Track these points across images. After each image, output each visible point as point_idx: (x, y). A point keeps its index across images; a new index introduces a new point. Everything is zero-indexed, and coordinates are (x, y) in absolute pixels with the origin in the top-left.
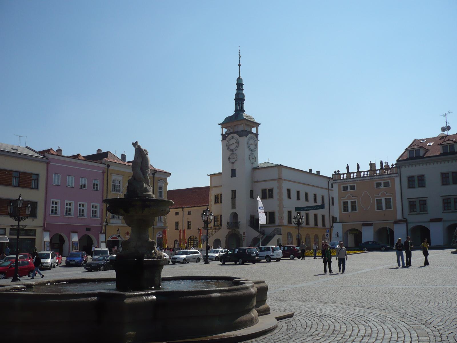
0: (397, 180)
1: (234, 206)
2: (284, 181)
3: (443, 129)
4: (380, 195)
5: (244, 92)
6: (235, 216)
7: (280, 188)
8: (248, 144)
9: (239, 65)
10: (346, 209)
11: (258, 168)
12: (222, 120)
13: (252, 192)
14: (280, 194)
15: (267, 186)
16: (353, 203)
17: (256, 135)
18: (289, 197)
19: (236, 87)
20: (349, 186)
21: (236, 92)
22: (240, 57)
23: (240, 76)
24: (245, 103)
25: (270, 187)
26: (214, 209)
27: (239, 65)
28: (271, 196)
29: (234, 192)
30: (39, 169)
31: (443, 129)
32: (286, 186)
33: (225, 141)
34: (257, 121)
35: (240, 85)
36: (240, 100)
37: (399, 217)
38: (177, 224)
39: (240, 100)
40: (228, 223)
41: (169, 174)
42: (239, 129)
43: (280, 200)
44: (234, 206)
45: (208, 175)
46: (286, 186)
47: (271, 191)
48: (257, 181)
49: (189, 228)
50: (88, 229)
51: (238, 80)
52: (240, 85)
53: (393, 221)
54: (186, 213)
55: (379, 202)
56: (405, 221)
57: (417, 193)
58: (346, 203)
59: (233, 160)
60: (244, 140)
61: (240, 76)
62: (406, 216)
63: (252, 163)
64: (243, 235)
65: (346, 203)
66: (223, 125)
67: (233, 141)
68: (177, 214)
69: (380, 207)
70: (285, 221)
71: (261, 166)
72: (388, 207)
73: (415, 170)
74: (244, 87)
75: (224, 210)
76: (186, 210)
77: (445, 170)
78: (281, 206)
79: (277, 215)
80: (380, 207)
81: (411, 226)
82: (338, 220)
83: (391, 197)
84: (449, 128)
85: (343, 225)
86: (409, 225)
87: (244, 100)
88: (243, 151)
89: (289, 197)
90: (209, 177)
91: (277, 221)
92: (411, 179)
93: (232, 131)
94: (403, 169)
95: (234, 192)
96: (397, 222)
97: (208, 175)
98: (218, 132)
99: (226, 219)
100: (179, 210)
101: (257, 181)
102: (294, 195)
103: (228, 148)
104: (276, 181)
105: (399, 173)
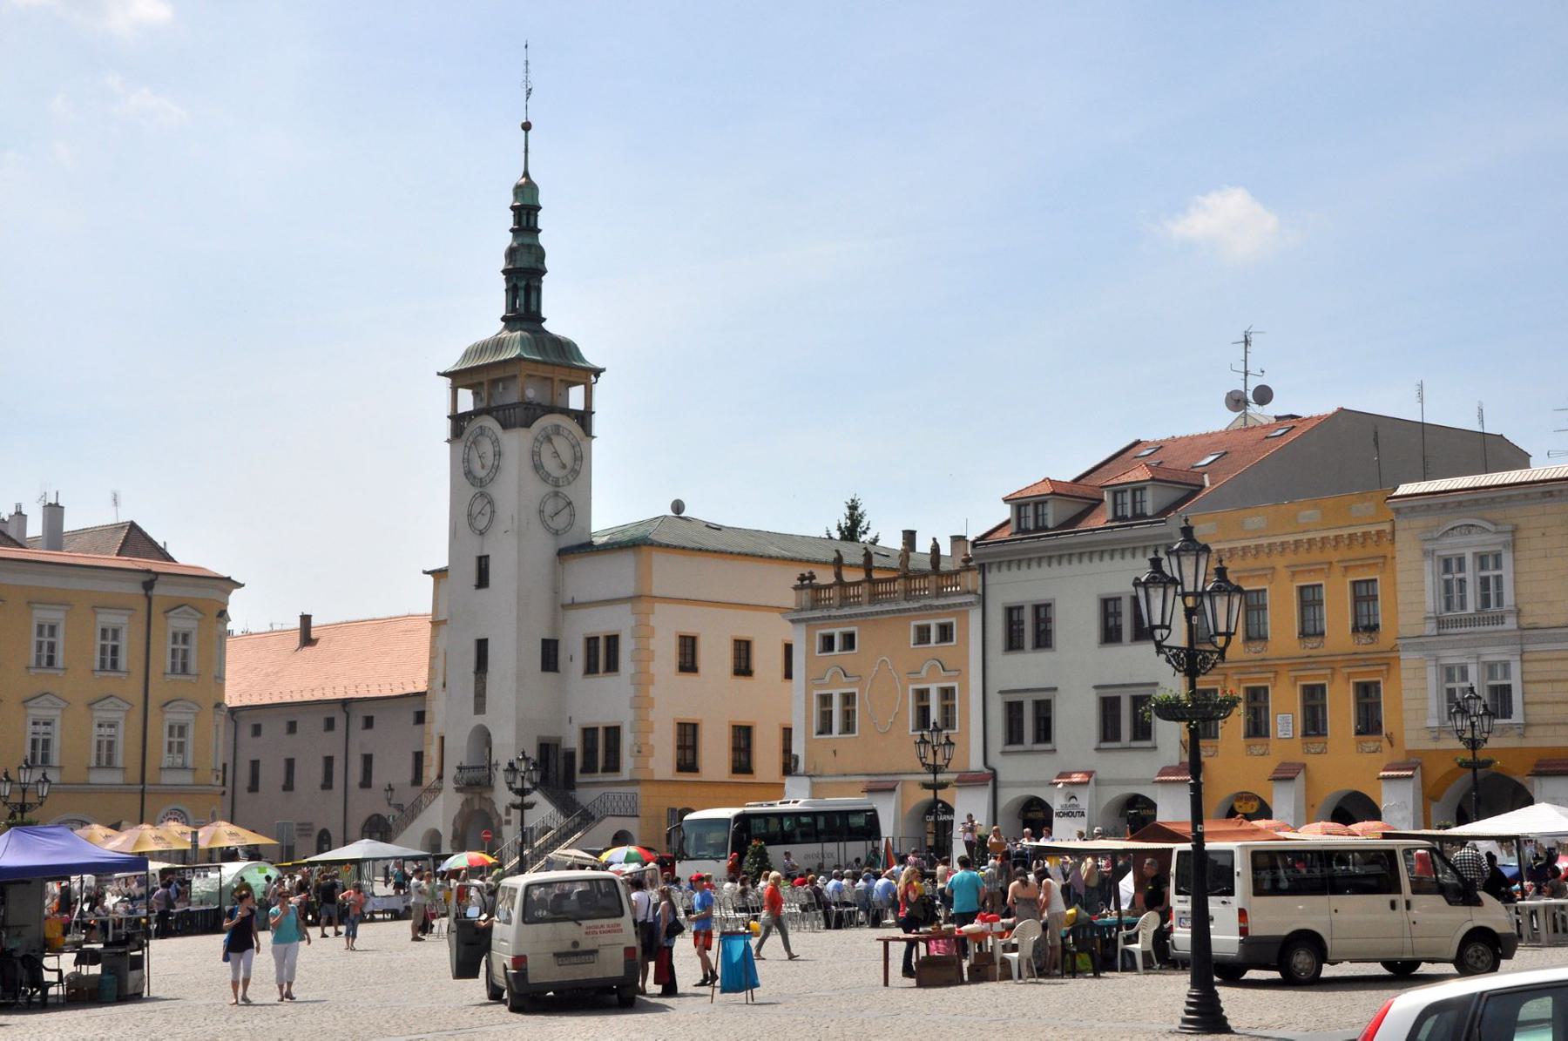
0: (975, 617)
2: (659, 607)
3: (1236, 401)
4: (924, 673)
5: (543, 239)
6: (483, 738)
7: (643, 633)
8: (535, 454)
9: (527, 127)
11: (587, 548)
12: (452, 362)
14: (644, 656)
15: (600, 623)
16: (848, 699)
17: (584, 419)
19: (509, 220)
20: (837, 633)
21: (507, 240)
22: (529, 92)
23: (526, 174)
24: (544, 287)
25: (610, 629)
27: (527, 127)
28: (612, 666)
29: (482, 645)
31: (1236, 401)
33: (460, 446)
34: (591, 357)
35: (526, 214)
36: (525, 274)
37: (976, 763)
39: (525, 274)
40: (460, 768)
41: (229, 584)
42: (523, 391)
43: (643, 680)
45: (426, 573)
47: (613, 641)
48: (574, 605)
49: (366, 783)
51: (518, 190)
52: (526, 214)
53: (955, 776)
56: (989, 779)
57: (1025, 671)
58: (826, 700)
59: (482, 523)
60: (516, 443)
61: (526, 174)
62: (996, 760)
63: (556, 533)
64: (504, 818)
65: (826, 700)
66: (458, 378)
68: (330, 724)
70: (663, 762)
71: (598, 541)
73: (1014, 587)
74: (543, 220)
78: (642, 703)
79: (627, 741)
81: (1008, 796)
82: (802, 767)
83: (911, 687)
84: (1264, 395)
85: (813, 785)
86: (1002, 792)
87: (544, 272)
88: (515, 487)
90: (430, 578)
93: (483, 405)
94: (993, 577)
95: (482, 645)
97: (426, 573)
98: (434, 406)
101: (574, 605)
102: (715, 656)
103: (469, 473)
104: (628, 607)
105: (980, 591)
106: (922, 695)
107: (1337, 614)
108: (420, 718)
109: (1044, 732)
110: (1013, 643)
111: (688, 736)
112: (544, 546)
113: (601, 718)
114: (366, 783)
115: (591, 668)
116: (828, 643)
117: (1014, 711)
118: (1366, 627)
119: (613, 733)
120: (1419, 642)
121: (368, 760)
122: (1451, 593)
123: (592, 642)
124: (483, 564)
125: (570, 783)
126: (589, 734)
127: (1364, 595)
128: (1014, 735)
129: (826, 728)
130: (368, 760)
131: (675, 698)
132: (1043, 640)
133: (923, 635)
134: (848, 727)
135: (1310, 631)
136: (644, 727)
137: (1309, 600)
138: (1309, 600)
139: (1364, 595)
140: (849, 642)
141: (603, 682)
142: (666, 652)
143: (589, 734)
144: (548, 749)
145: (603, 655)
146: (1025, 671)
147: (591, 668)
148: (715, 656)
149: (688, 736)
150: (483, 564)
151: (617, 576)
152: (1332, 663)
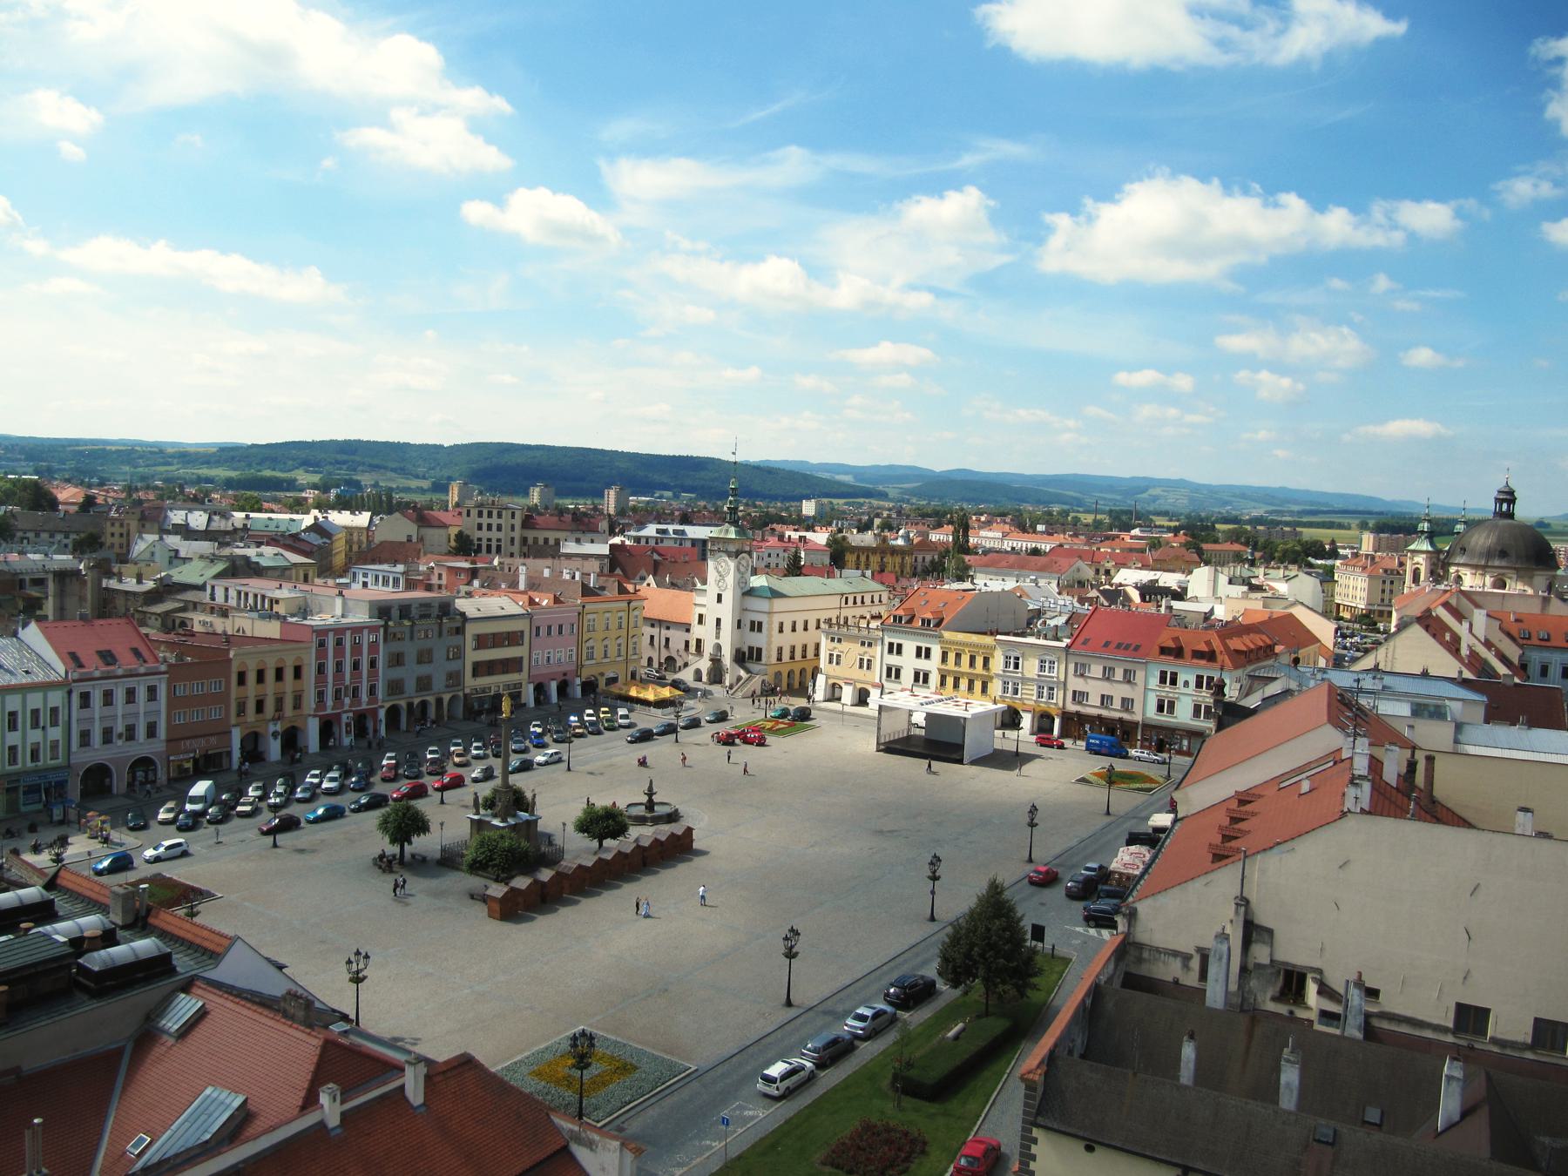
1: (718, 637)
6: (718, 647)
7: (770, 623)
10: (831, 662)
14: (770, 629)
15: (757, 618)
18: (781, 631)
26: (698, 631)
28: (760, 630)
29: (718, 621)
30: (522, 625)
32: (777, 619)
43: (770, 636)
44: (718, 637)
46: (777, 619)
47: (760, 624)
57: (893, 660)
70: (774, 660)
75: (704, 632)
78: (769, 643)
80: (861, 667)
89: (781, 631)
92: (891, 645)
95: (718, 621)
96: (875, 686)
99: (708, 649)
108: (688, 630)
109: (898, 676)
110: (890, 651)
111: (780, 650)
112: (739, 593)
113: (756, 645)
114: (667, 645)
115: (752, 629)
117: (889, 670)
119: (759, 650)
120: (998, 675)
121: (667, 640)
122: (1007, 665)
123: (753, 623)
127: (986, 661)
128: (889, 675)
130: (667, 640)
131: (778, 640)
132: (899, 652)
136: (769, 651)
137: (972, 659)
138: (972, 659)
139: (986, 661)
141: (755, 634)
142: (776, 627)
143: (751, 649)
145: (757, 627)
146: (893, 660)
147: (752, 629)
148: (787, 627)
149: (780, 650)
151: (762, 605)
152: (977, 676)
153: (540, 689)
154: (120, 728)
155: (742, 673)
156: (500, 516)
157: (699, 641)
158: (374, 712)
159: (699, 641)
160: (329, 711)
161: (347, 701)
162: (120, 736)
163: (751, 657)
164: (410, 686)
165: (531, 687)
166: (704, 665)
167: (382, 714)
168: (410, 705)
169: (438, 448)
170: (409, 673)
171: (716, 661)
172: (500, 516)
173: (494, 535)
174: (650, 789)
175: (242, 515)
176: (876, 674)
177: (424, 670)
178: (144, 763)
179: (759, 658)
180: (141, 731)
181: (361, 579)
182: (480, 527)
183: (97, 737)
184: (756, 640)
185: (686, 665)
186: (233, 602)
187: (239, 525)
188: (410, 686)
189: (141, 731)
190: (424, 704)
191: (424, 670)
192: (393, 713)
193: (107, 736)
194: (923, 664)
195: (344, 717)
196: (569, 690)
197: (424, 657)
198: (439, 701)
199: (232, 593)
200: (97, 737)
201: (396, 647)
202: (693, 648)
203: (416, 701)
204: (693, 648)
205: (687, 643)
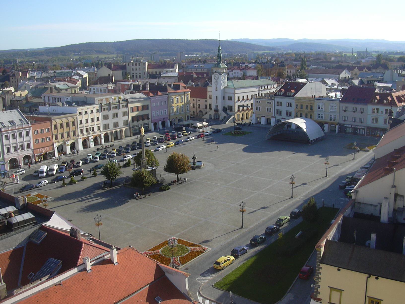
1: (217, 102)
6: (217, 106)
13: (224, 97)
26: (209, 101)
29: (217, 97)
37: (273, 116)
38: (194, 105)
44: (217, 102)
46: (236, 96)
47: (231, 97)
50: (164, 119)
54: (198, 100)
55: (268, 108)
56: (275, 117)
57: (279, 108)
58: (257, 107)
65: (257, 107)
67: (216, 76)
69: (268, 111)
72: (270, 111)
76: (198, 99)
77: (288, 102)
80: (268, 111)
91: (233, 110)
92: (278, 102)
95: (217, 97)
96: (272, 117)
99: (214, 107)
100: (195, 99)
106: (268, 108)
107: (309, 108)
109: (281, 113)
113: (230, 105)
114: (199, 108)
116: (257, 102)
117: (277, 111)
118: (311, 109)
119: (232, 107)
123: (229, 97)
124: (216, 88)
125: (226, 111)
126: (228, 106)
128: (277, 113)
129: (257, 110)
130: (199, 105)
132: (281, 105)
133: (268, 103)
134: (259, 110)
135: (307, 109)
139: (311, 107)
140: (260, 102)
141: (230, 101)
143: (228, 106)
144: (224, 107)
146: (279, 108)
147: (229, 99)
150: (216, 88)
153: (155, 124)
154: (19, 146)
155: (226, 115)
156: (139, 65)
157: (210, 105)
158: (100, 136)
159: (210, 105)
160: (86, 136)
161: (91, 132)
162: (19, 149)
163: (229, 109)
164: (111, 126)
165: (152, 124)
166: (212, 113)
167: (103, 136)
168: (111, 133)
169: (74, 45)
170: (111, 121)
171: (217, 110)
172: (139, 65)
173: (138, 72)
174: (194, 157)
175: (53, 71)
176: (273, 113)
177: (115, 120)
178: (27, 157)
179: (231, 110)
180: (26, 147)
181: (93, 90)
182: (133, 69)
183: (12, 149)
184: (229, 103)
185: (206, 113)
186: (51, 101)
187: (52, 75)
188: (111, 126)
189: (26, 147)
190: (116, 132)
191: (115, 120)
192: (106, 136)
193: (15, 149)
194: (289, 109)
195: (90, 138)
196: (166, 124)
197: (116, 116)
198: (121, 131)
199: (51, 98)
200: (12, 149)
201: (106, 113)
202: (208, 107)
203: (114, 131)
204: (208, 107)
205: (206, 106)
